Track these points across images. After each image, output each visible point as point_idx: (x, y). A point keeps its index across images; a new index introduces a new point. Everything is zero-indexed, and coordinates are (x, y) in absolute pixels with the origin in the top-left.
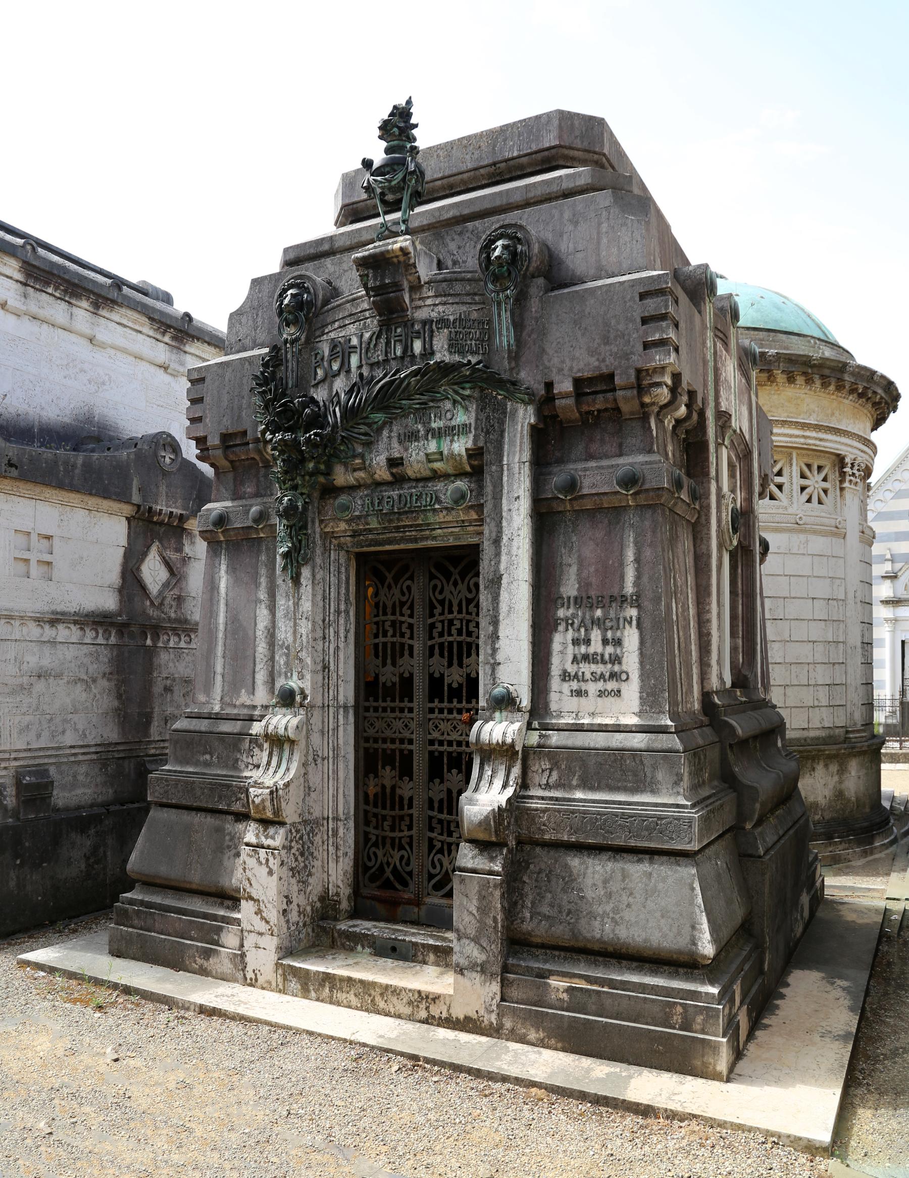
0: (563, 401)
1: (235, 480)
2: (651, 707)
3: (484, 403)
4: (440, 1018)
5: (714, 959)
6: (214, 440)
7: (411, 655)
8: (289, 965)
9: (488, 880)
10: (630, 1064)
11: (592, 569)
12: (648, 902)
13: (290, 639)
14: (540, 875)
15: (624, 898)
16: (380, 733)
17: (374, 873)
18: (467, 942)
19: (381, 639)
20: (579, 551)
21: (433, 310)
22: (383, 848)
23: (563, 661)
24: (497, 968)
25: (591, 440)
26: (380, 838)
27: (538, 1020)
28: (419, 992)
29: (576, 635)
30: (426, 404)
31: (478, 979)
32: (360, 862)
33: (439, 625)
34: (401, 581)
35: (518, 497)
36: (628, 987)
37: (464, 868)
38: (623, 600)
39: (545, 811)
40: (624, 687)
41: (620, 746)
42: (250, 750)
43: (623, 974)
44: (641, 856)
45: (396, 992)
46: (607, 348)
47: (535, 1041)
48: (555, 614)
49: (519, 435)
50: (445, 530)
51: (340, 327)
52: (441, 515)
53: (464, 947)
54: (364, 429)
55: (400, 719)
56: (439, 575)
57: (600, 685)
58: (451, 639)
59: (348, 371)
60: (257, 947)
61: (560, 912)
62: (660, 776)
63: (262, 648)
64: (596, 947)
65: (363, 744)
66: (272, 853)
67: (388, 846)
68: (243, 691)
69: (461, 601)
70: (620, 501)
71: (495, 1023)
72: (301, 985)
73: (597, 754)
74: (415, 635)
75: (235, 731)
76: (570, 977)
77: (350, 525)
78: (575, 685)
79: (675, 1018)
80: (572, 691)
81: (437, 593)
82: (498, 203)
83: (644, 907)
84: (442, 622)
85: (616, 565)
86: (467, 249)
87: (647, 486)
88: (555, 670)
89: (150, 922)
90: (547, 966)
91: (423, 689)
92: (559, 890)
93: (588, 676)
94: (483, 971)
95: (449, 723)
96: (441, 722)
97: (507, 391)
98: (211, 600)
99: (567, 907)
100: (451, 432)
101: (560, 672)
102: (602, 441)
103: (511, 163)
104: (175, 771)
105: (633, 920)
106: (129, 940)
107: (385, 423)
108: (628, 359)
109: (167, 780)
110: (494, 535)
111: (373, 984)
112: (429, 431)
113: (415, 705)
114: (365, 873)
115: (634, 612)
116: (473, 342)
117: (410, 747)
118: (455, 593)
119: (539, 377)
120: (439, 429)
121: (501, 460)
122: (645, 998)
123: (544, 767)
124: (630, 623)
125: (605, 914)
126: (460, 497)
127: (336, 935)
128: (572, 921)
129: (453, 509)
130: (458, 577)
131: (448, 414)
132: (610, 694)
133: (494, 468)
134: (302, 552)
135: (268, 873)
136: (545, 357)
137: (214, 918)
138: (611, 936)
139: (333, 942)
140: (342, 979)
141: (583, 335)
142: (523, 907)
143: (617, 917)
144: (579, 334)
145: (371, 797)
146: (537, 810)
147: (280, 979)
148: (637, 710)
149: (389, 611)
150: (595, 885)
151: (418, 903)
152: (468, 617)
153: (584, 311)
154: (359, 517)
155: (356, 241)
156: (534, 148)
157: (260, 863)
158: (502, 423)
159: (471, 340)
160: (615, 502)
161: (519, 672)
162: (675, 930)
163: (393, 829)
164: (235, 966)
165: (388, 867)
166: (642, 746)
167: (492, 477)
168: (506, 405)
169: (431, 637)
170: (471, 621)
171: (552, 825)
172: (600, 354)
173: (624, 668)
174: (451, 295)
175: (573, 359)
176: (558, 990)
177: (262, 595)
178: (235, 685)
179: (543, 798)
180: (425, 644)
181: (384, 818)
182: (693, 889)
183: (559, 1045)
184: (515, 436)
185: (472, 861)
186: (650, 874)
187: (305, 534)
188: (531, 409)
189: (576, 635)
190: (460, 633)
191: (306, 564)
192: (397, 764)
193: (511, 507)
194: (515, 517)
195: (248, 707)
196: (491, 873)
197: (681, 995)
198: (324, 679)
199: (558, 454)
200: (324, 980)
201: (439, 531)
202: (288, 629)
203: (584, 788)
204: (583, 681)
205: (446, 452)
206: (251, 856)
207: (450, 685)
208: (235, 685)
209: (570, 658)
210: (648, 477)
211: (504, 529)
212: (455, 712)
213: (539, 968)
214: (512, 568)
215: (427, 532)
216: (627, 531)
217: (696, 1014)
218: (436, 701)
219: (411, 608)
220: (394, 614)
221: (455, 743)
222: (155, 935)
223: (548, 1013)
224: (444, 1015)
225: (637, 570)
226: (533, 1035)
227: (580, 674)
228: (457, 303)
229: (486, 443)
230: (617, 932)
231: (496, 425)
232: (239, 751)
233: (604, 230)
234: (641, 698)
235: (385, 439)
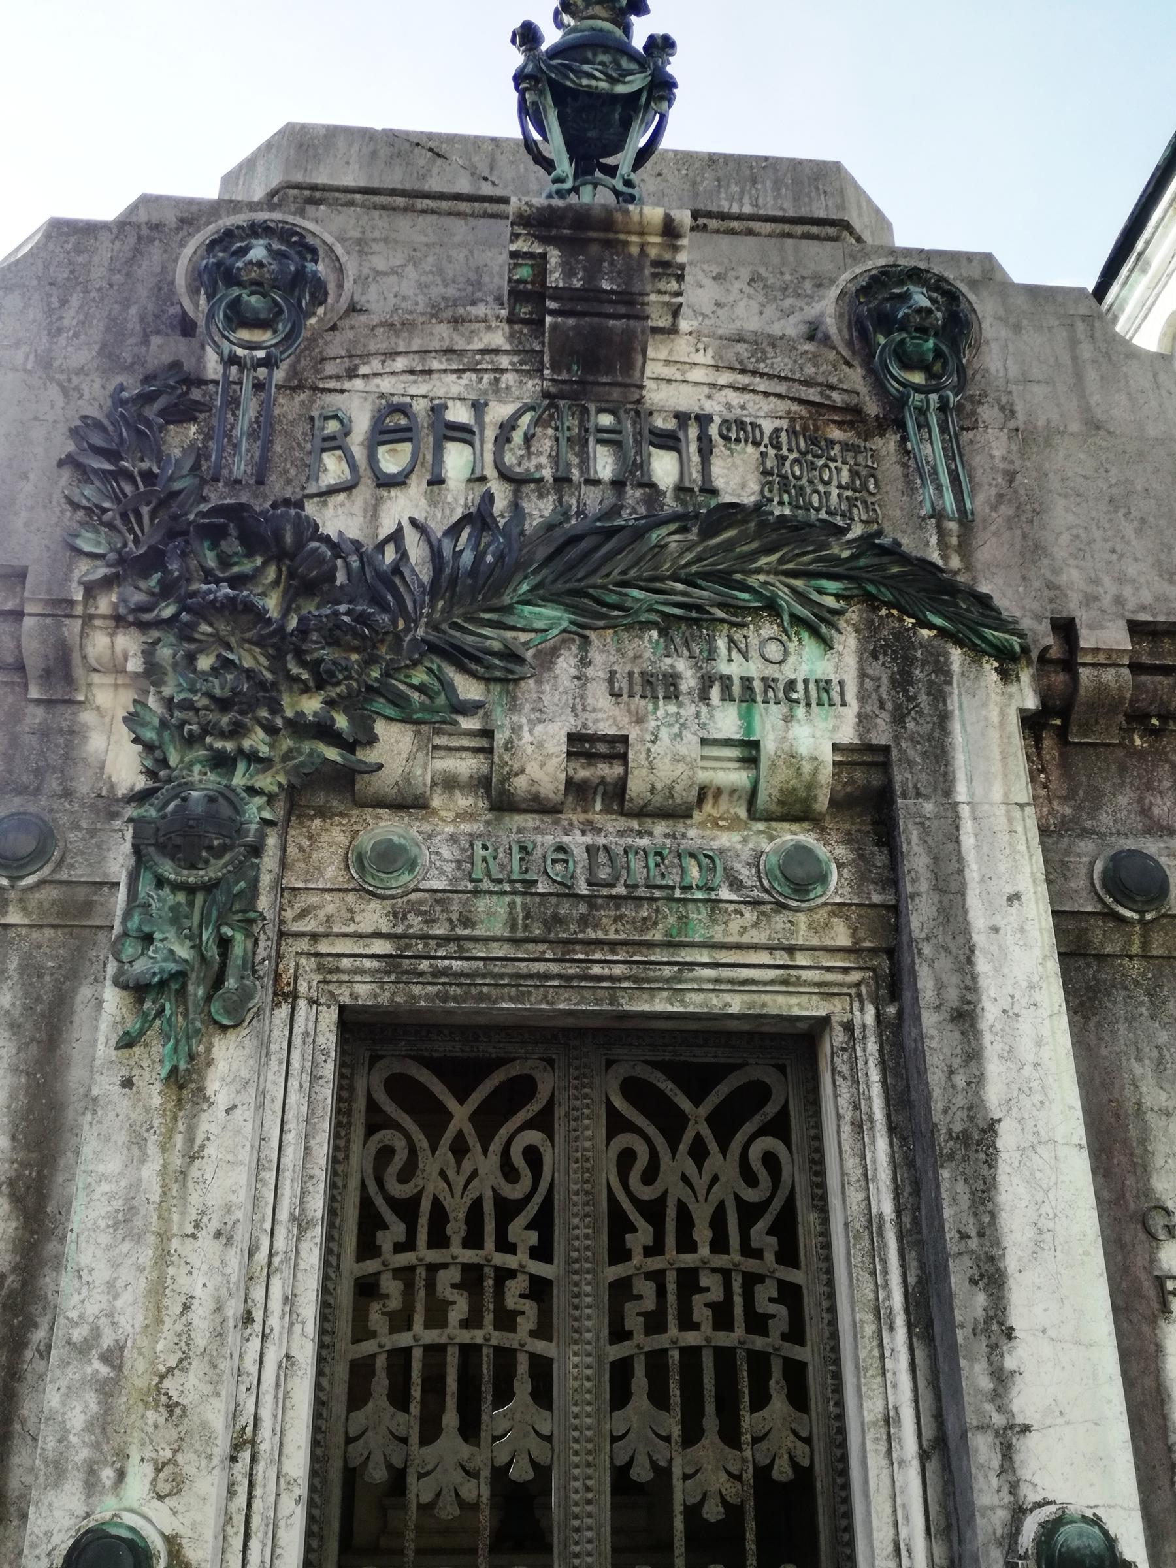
7: (543, 1395)
21: (709, 397)
34: (504, 1132)
48: (1153, 1261)
51: (412, 372)
56: (640, 1120)
58: (691, 1339)
59: (437, 481)
81: (634, 1180)
84: (658, 1277)
110: (952, 996)
118: (701, 1184)
121: (948, 792)
130: (706, 1132)
133: (929, 807)
134: (231, 983)
141: (1139, 531)
144: (1129, 530)
149: (456, 1229)
152: (751, 1265)
159: (826, 483)
168: (946, 655)
169: (619, 1334)
174: (762, 375)
175: (1121, 579)
190: (722, 1317)
193: (999, 921)
198: (231, 1493)
202: (126, 1274)
205: (769, 746)
211: (983, 982)
214: (1025, 1102)
219: (543, 1223)
228: (779, 396)
229: (897, 738)
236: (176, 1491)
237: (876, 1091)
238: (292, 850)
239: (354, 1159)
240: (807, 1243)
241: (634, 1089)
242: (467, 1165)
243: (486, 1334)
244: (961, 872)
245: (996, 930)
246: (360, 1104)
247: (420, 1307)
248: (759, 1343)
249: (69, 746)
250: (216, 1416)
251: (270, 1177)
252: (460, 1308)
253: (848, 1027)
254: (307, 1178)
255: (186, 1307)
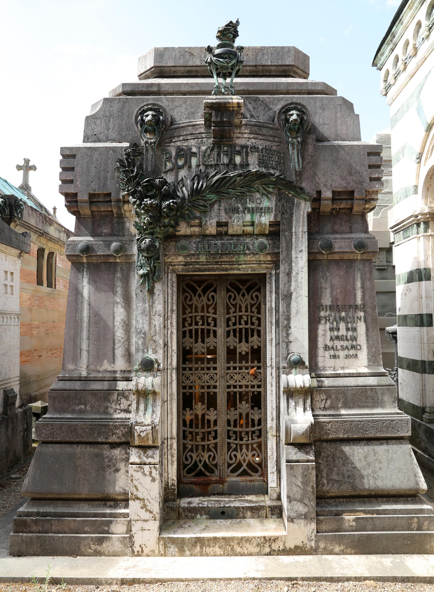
0: (326, 202)
1: (93, 223)
2: (374, 363)
3: (280, 197)
4: (279, 550)
5: (427, 491)
6: (83, 197)
7: (215, 336)
8: (169, 538)
9: (308, 465)
10: (393, 554)
11: (339, 291)
12: (390, 465)
13: (146, 328)
14: (328, 458)
15: (377, 465)
16: (206, 383)
17: (190, 468)
18: (295, 502)
19: (194, 327)
20: (331, 281)
22: (196, 452)
23: (324, 340)
24: (314, 515)
25: (335, 223)
26: (194, 446)
27: (340, 540)
28: (264, 537)
29: (331, 326)
30: (244, 193)
31: (302, 523)
32: (181, 462)
33: (233, 319)
34: (208, 293)
35: (302, 251)
36: (387, 512)
37: (291, 460)
38: (356, 307)
39: (329, 422)
40: (359, 353)
41: (364, 384)
42: (118, 400)
43: (380, 506)
44: (381, 441)
45: (248, 540)
46: (351, 177)
47: (338, 552)
49: (302, 217)
50: (248, 265)
52: (249, 257)
53: (293, 506)
54: (202, 203)
55: (207, 374)
56: (233, 290)
57: (346, 352)
58: (241, 327)
60: (143, 529)
61: (344, 477)
62: (386, 398)
63: (119, 333)
64: (365, 493)
65: (182, 391)
66: (155, 467)
67: (200, 450)
68: (106, 361)
69: (247, 305)
70: (354, 256)
71: (314, 546)
72: (179, 548)
73: (352, 389)
74: (218, 324)
75: (105, 388)
76: (355, 512)
77: (185, 259)
78: (332, 352)
79: (414, 525)
80: (330, 356)
81: (231, 300)
82: (271, 88)
83: (389, 468)
84: (235, 317)
85: (352, 289)
86: (259, 110)
87: (369, 250)
88: (321, 345)
89: (47, 526)
90: (339, 508)
91: (224, 356)
92: (341, 465)
93: (339, 347)
94: (306, 518)
95: (240, 375)
96: (235, 375)
97: (296, 192)
98: (76, 301)
99: (347, 474)
100: (261, 211)
101: (323, 346)
102: (341, 225)
103: (266, 68)
104: (57, 418)
105: (384, 476)
106: (29, 542)
107: (216, 201)
108: (362, 185)
109: (52, 425)
110: (287, 271)
111: (233, 539)
112: (245, 208)
113: (218, 365)
114: (184, 468)
115: (362, 314)
116: (274, 163)
117: (215, 390)
118: (243, 301)
119: (313, 187)
120: (253, 208)
122: (398, 517)
123: (322, 398)
124: (360, 320)
125: (369, 475)
126: (262, 248)
127: (181, 511)
128: (351, 481)
129: (257, 254)
131: (258, 200)
132: (351, 357)
133: (287, 233)
134: (157, 274)
135: (151, 480)
136: (316, 177)
137: (104, 515)
138: (374, 486)
139: (179, 516)
140: (209, 539)
142: (322, 477)
143: (375, 475)
144: (336, 168)
145: (188, 423)
146: (324, 422)
147: (162, 548)
148: (366, 365)
149: (199, 310)
150: (360, 460)
151: (222, 481)
152: (252, 314)
153: (338, 156)
154: (193, 255)
155: (177, 90)
156: (280, 63)
157: (145, 475)
158: (292, 209)
160: (351, 257)
161: (303, 346)
162: (406, 478)
163: (203, 439)
164: (125, 545)
165: (200, 463)
166: (375, 383)
167: (286, 238)
169: (228, 326)
170: (253, 316)
171: (333, 430)
172: (347, 180)
173: (359, 343)
175: (332, 180)
176: (349, 520)
177: (119, 299)
178: (98, 358)
179: (325, 415)
180: (225, 330)
181: (197, 434)
182: (411, 456)
183: (353, 551)
184: (299, 217)
185: (295, 456)
186: (388, 450)
187: (159, 263)
188: (308, 204)
189: (331, 326)
190: (246, 323)
191: (159, 281)
192: (206, 401)
193: (298, 256)
194: (300, 261)
195: (110, 372)
196: (308, 461)
197: (414, 512)
198: (164, 352)
199: (316, 229)
200: (196, 543)
201: (244, 266)
202: (145, 321)
203: (345, 408)
204: (337, 350)
205: (256, 222)
206: (137, 471)
207: (240, 353)
208: (98, 358)
209: (329, 338)
210: (370, 245)
211: (293, 268)
212: (244, 369)
213: (336, 510)
215: (236, 266)
216: (356, 272)
217: (424, 521)
218: (232, 362)
219: (215, 308)
220: (203, 311)
221: (244, 387)
222: (52, 535)
223: (345, 535)
224: (281, 548)
225: (363, 292)
226: (337, 549)
227: (335, 346)
229: (282, 219)
230: (377, 484)
231: (288, 210)
232: (109, 401)
233: (339, 116)
234: (368, 358)
235: (216, 210)
236: (156, 353)
237: (274, 286)
238: (165, 246)
239: (181, 298)
240: (262, 310)
241: (231, 284)
242: (201, 299)
243: (205, 327)
244: (291, 246)
245: (297, 257)
246: (181, 289)
247: (194, 322)
248: (252, 327)
249: (123, 226)
250: (161, 342)
251: (166, 304)
252: (200, 323)
253: (271, 274)
254: (172, 303)
255: (155, 326)
